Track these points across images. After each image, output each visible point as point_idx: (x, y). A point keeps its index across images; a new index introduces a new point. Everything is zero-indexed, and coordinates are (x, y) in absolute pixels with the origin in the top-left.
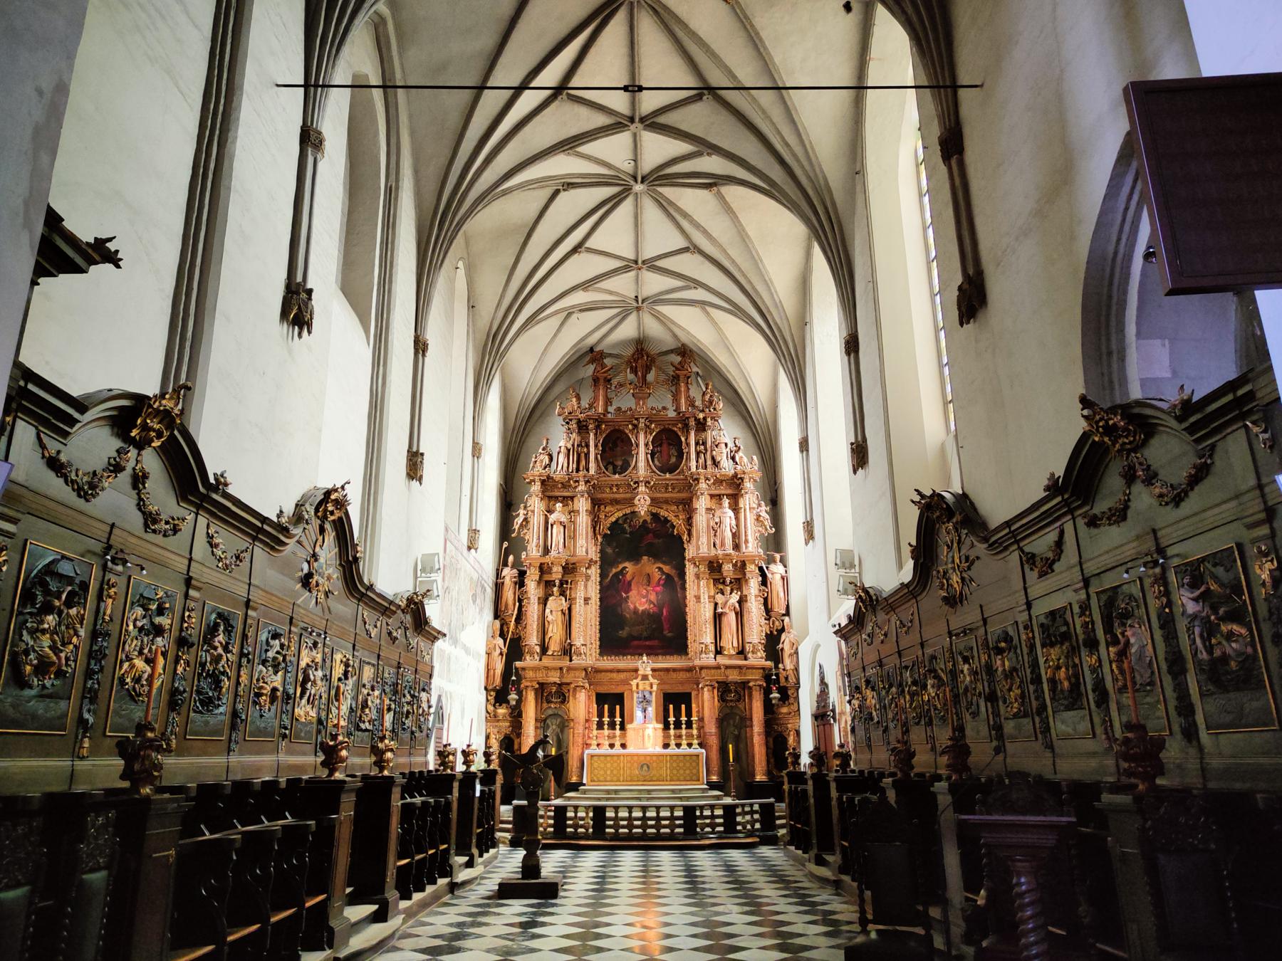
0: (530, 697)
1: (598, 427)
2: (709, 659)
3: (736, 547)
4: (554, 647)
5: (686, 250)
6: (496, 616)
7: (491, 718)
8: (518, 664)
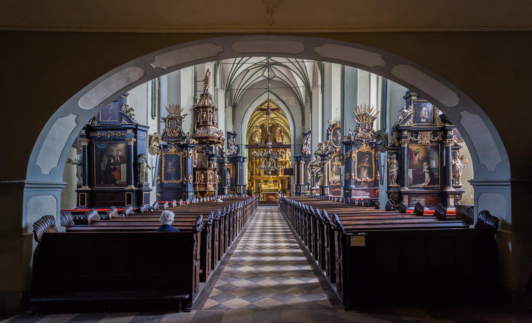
0: (254, 181)
1: (264, 139)
2: (280, 176)
3: (285, 159)
4: (257, 174)
5: (277, 117)
6: (249, 169)
7: (249, 184)
8: (252, 176)
